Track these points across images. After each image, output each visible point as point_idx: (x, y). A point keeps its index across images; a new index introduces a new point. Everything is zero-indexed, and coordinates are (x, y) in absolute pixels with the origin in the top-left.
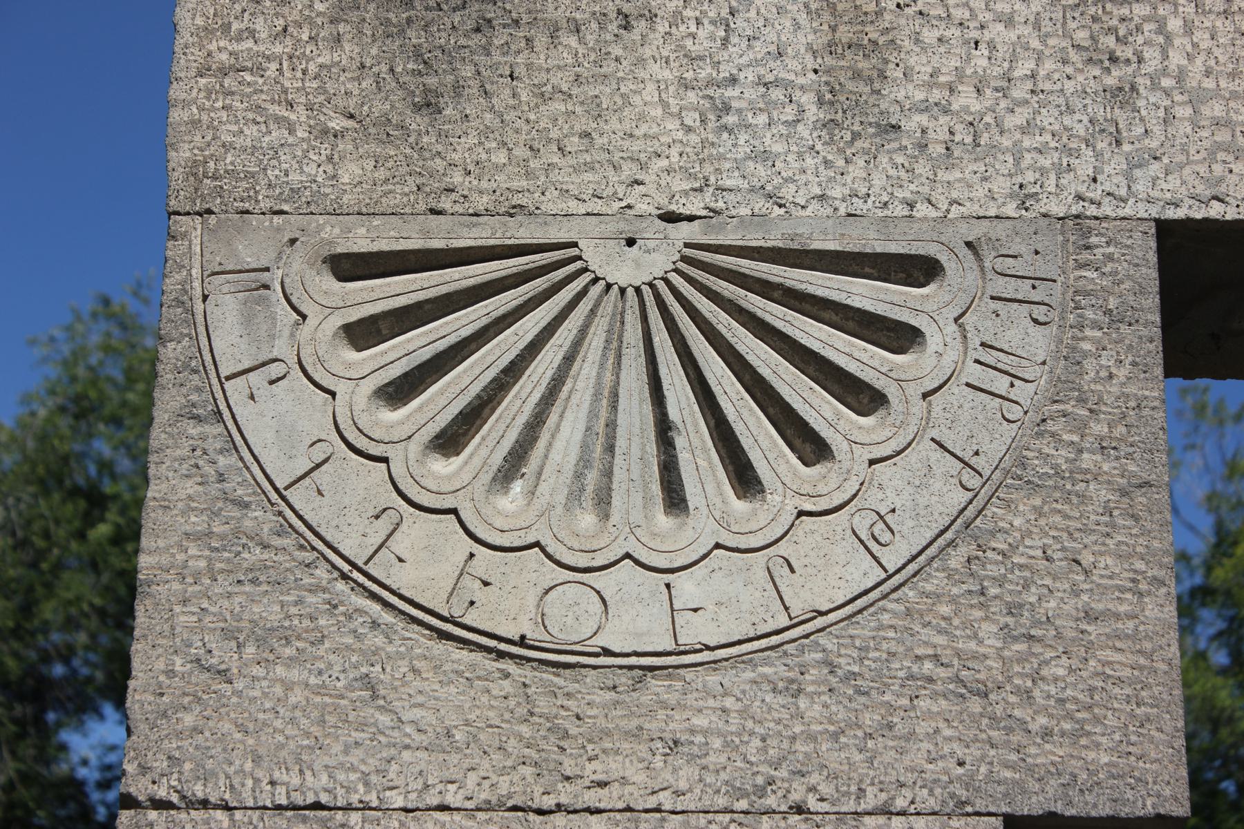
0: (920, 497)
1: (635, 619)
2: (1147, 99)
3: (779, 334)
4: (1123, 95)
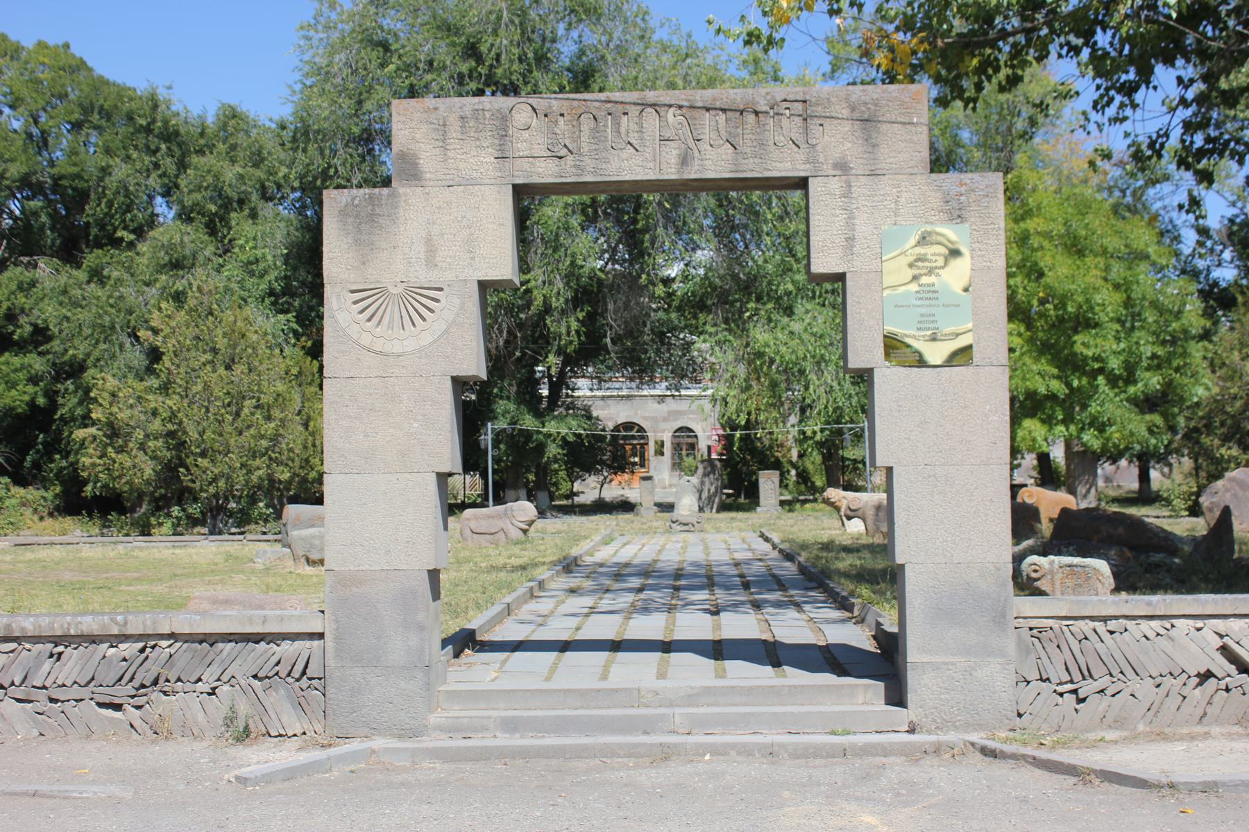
1: (397, 348)
2: (477, 259)
3: (421, 299)
4: (473, 258)
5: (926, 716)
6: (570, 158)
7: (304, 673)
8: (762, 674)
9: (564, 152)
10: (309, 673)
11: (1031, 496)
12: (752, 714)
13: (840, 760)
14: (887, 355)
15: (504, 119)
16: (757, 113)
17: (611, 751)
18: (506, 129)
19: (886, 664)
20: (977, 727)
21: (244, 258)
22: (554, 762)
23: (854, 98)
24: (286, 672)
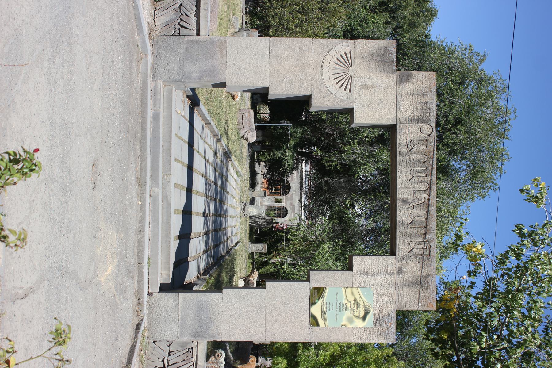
0: (333, 90)
1: (325, 71)
3: (346, 82)
4: (364, 106)
5: (155, 300)
6: (407, 150)
7: (182, 26)
8: (176, 230)
9: (410, 147)
10: (182, 29)
11: (252, 361)
12: (158, 224)
13: (137, 261)
14: (315, 288)
15: (426, 121)
16: (425, 234)
17: (143, 160)
18: (421, 122)
19: (177, 284)
20: (150, 323)
21: (369, 18)
22: (139, 135)
24: (183, 19)
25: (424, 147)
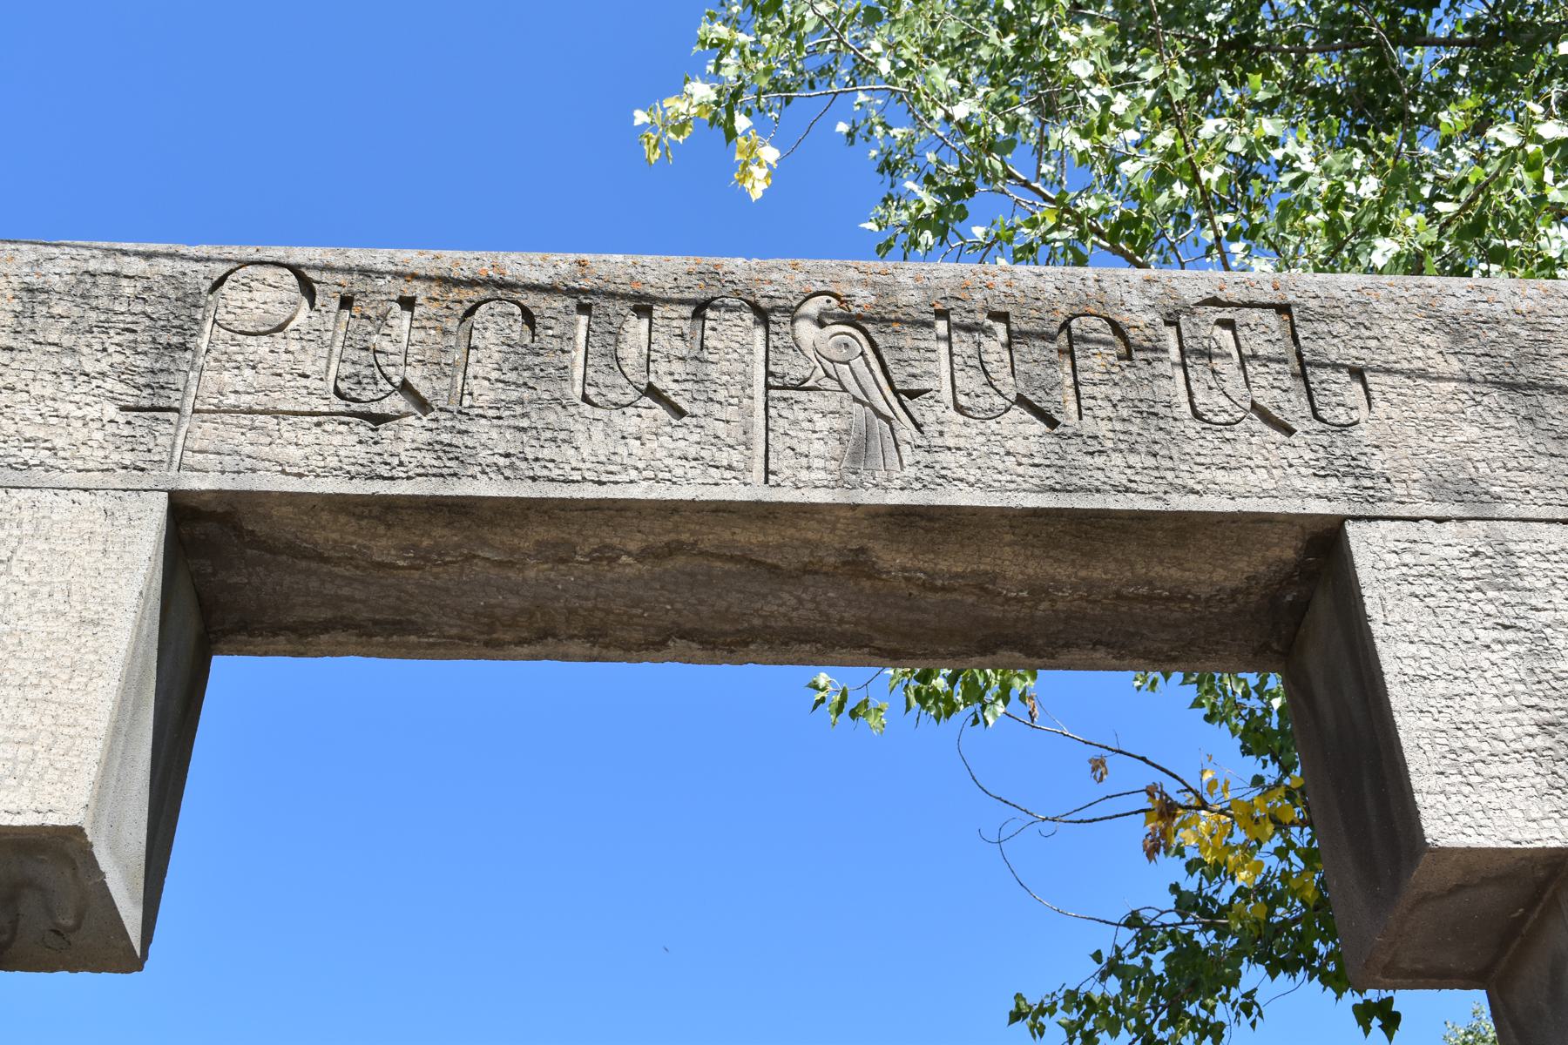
9: (397, 403)
23: (1450, 306)
25: (402, 322)
